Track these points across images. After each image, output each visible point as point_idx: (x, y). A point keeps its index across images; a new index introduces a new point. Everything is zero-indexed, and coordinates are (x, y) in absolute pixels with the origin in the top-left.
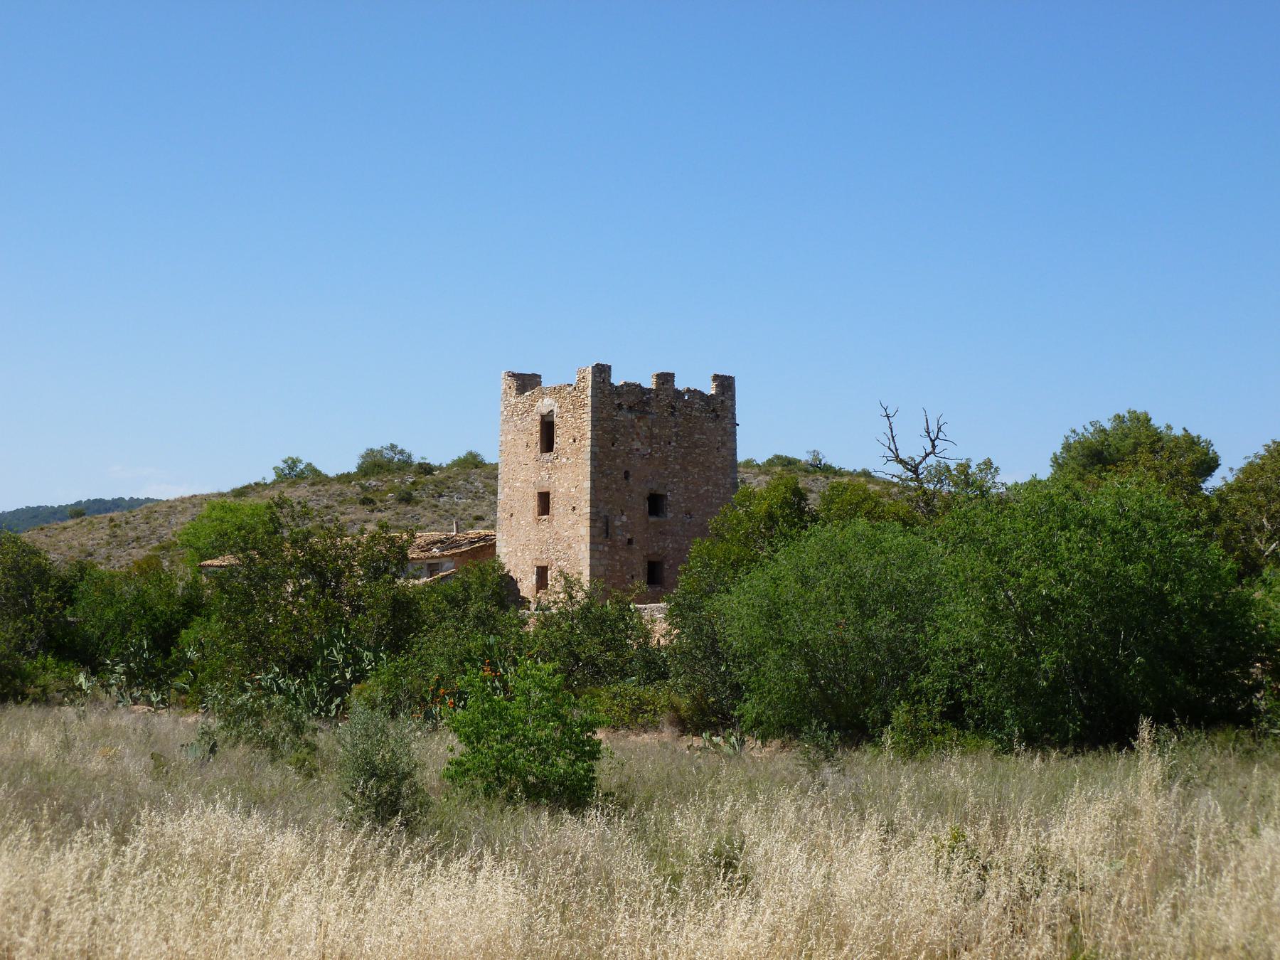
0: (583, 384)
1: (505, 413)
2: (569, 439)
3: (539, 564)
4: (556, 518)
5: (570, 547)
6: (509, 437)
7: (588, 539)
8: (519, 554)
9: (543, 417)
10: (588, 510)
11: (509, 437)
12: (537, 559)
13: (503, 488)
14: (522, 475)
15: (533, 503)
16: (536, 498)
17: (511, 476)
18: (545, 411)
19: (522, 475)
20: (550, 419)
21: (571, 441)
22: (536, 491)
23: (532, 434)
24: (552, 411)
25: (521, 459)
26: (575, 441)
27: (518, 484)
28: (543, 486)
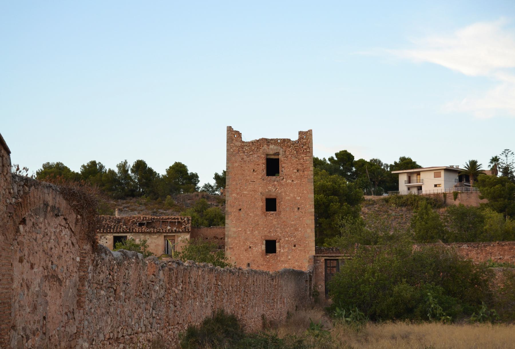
0: (305, 140)
1: (231, 150)
2: (293, 170)
3: (268, 238)
4: (282, 213)
5: (296, 230)
6: (237, 165)
7: (313, 226)
8: (249, 233)
9: (267, 155)
10: (313, 210)
11: (237, 165)
12: (266, 236)
13: (231, 194)
14: (250, 187)
15: (261, 204)
16: (265, 201)
17: (238, 187)
18: (271, 152)
19: (250, 187)
20: (276, 157)
21: (296, 171)
22: (264, 198)
23: (258, 165)
24: (279, 153)
25: (248, 178)
26: (298, 171)
27: (245, 192)
28: (270, 195)
